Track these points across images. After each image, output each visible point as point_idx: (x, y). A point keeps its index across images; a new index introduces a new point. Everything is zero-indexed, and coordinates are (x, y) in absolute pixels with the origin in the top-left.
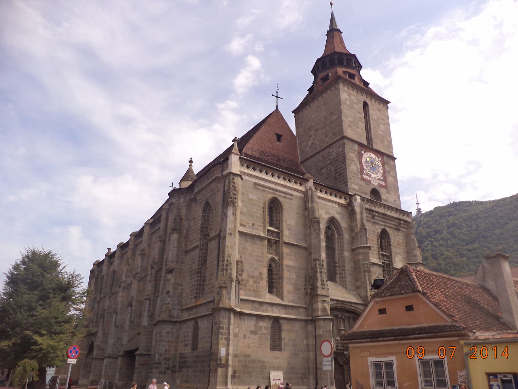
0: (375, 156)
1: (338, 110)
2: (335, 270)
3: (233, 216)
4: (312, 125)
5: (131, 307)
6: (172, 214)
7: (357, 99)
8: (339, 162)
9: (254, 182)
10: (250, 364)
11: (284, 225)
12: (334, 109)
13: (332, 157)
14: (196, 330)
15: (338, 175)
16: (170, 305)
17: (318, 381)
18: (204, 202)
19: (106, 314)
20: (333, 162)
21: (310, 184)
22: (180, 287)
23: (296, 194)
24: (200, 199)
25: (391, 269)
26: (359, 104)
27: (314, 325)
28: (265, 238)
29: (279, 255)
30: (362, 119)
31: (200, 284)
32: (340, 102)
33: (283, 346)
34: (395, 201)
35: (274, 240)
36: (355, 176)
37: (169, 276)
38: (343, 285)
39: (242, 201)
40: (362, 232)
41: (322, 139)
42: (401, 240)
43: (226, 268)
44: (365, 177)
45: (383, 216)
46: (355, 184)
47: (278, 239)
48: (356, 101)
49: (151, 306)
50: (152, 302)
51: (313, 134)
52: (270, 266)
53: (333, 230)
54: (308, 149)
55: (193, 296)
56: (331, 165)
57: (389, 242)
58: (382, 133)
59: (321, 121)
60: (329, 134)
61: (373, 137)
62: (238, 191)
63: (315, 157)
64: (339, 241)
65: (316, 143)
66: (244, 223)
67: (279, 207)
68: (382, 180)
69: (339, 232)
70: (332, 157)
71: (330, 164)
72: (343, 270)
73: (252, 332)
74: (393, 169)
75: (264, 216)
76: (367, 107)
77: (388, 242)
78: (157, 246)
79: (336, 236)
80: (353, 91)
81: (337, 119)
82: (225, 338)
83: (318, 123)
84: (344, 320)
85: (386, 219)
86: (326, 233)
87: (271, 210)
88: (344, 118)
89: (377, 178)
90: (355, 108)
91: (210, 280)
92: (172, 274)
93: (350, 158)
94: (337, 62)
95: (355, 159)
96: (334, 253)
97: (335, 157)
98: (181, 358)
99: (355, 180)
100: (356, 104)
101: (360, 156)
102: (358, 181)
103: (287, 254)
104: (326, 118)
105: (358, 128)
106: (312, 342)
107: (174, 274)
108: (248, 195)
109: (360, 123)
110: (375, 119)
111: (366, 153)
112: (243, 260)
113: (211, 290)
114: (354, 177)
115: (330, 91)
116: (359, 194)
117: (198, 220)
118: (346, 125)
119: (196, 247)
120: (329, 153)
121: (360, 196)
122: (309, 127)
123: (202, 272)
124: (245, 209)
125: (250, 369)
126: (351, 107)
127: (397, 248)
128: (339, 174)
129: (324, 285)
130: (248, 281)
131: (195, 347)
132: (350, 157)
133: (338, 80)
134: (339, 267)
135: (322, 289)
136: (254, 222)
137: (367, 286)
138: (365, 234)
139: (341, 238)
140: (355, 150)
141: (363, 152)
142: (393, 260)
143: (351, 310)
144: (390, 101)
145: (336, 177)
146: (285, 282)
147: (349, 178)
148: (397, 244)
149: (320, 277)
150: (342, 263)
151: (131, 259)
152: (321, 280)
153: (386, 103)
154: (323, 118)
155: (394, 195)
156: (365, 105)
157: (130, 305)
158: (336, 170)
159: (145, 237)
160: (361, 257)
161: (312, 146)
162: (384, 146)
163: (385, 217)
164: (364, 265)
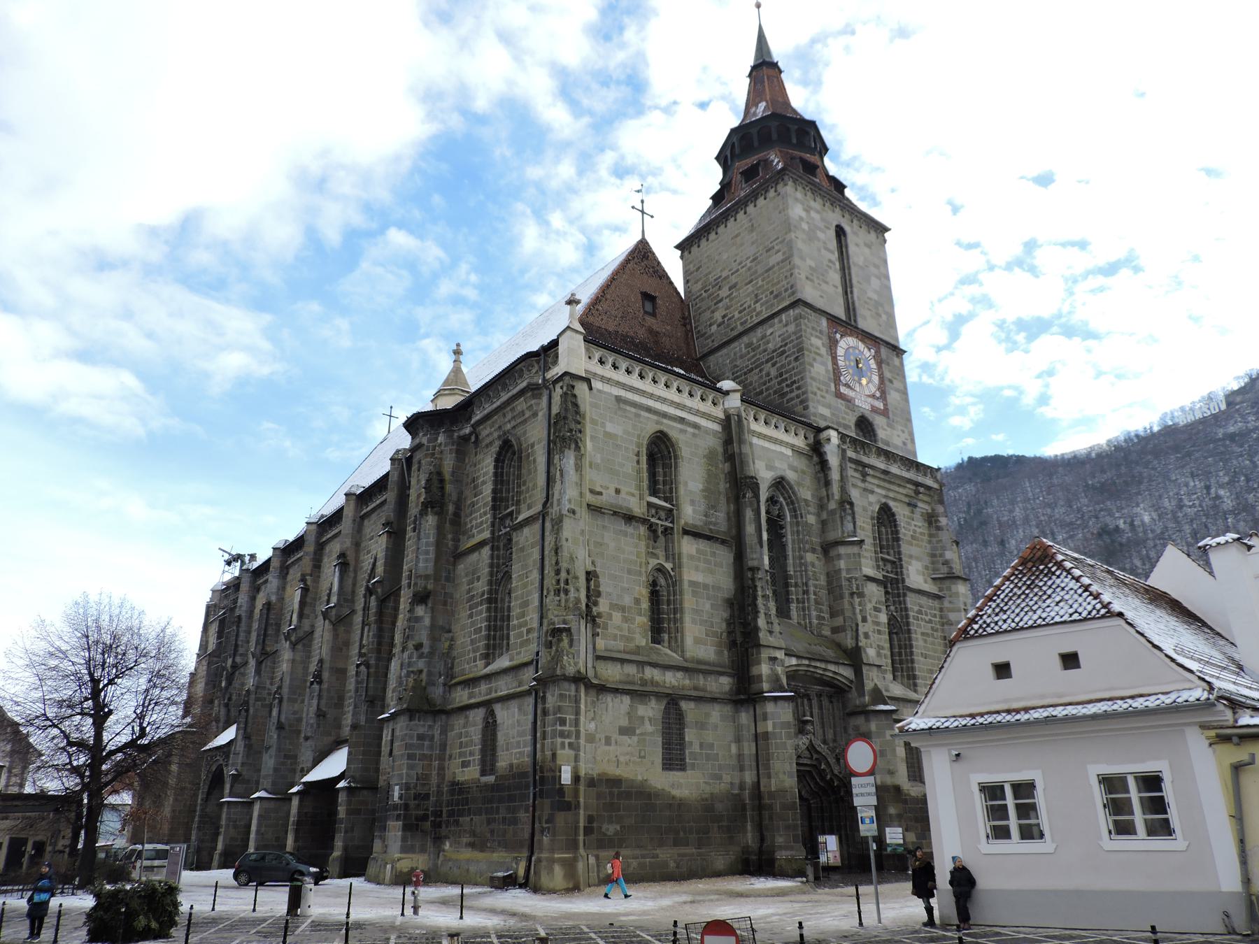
0: (863, 346)
1: (781, 242)
2: (788, 593)
3: (577, 471)
4: (723, 276)
5: (320, 683)
6: (419, 470)
7: (823, 220)
8: (787, 357)
9: (616, 396)
10: (622, 802)
11: (682, 491)
12: (775, 240)
13: (770, 345)
14: (490, 727)
15: (787, 386)
16: (424, 676)
17: (765, 833)
18: (498, 443)
19: (251, 702)
20: (772, 358)
21: (734, 402)
22: (446, 635)
23: (705, 425)
24: (488, 435)
25: (901, 591)
26: (828, 231)
27: (752, 712)
28: (644, 521)
29: (674, 559)
30: (834, 264)
31: (495, 626)
32: (789, 224)
33: (687, 760)
34: (904, 444)
35: (662, 526)
36: (824, 388)
37: (420, 611)
38: (806, 623)
39: (592, 437)
40: (845, 510)
41: (746, 305)
42: (920, 527)
43: (566, 587)
44: (843, 390)
45: (882, 476)
46: (823, 406)
47: (671, 525)
48: (821, 225)
49: (372, 679)
50: (372, 670)
51: (725, 295)
52: (654, 584)
53: (781, 505)
54: (714, 328)
55: (478, 654)
56: (770, 364)
57: (897, 532)
58: (875, 297)
59: (743, 267)
60: (764, 296)
62: (584, 415)
63: (733, 345)
64: (795, 529)
65: (733, 316)
66: (598, 489)
67: (669, 452)
68: (878, 398)
69: (795, 511)
70: (771, 346)
71: (767, 361)
72: (804, 594)
73: (624, 731)
74: (898, 375)
75: (639, 472)
76: (843, 238)
77: (892, 531)
78: (377, 546)
79: (789, 519)
80: (815, 200)
81: (783, 261)
82: (570, 744)
83: (738, 270)
84: (809, 700)
85: (890, 482)
86: (768, 512)
87: (652, 458)
88: (796, 260)
90: (819, 240)
91: (523, 615)
92: (426, 605)
93: (813, 349)
94: (775, 136)
95: (823, 351)
96: (785, 557)
97: (779, 346)
98: (452, 792)
99: (822, 396)
101: (833, 344)
102: (831, 399)
103: (691, 557)
104: (754, 260)
106: (749, 749)
107: (430, 605)
108: (603, 425)
109: (829, 270)
110: (861, 264)
111: (845, 339)
112: (598, 570)
113: (525, 638)
114: (822, 391)
115: (765, 199)
116: (835, 427)
117: (484, 483)
118: (803, 276)
119: (481, 544)
120: (764, 337)
121: (837, 430)
122: (715, 280)
123: (499, 599)
124: (599, 456)
125: (622, 813)
126: (811, 237)
127: (912, 545)
128: (789, 382)
129: (772, 623)
130: (610, 616)
131: (488, 764)
132: (811, 345)
133: (784, 175)
134: (796, 585)
135: (768, 634)
136: (618, 487)
137: (857, 625)
138: (849, 514)
139: (798, 524)
140: (821, 332)
141: (838, 336)
142: (905, 571)
143: (825, 678)
144: (889, 227)
145: (783, 387)
146: (687, 619)
147: (812, 393)
149: (763, 607)
150: (802, 579)
151: (311, 575)
152: (766, 614)
153: (881, 229)
154: (748, 261)
155: (903, 432)
156: (840, 232)
157: (318, 678)
158: (781, 375)
159: (346, 525)
160: (842, 564)
161: (724, 322)
162: (880, 326)
163: (887, 478)
164: (849, 580)
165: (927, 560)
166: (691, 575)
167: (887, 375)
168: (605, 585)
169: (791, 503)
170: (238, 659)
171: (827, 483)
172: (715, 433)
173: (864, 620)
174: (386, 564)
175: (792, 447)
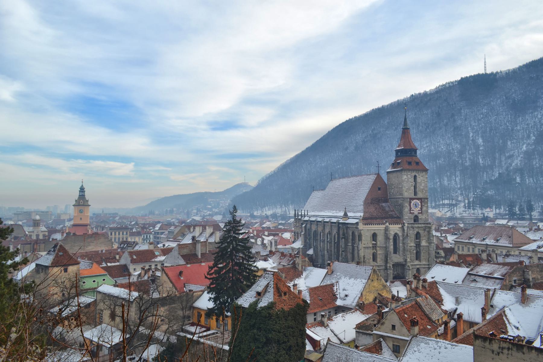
11: (378, 240)
21: (387, 224)
37: (343, 253)
44: (411, 212)
86: (394, 238)
89: (417, 210)
95: (408, 205)
100: (410, 179)
101: (410, 203)
102: (408, 215)
106: (386, 275)
160: (405, 246)
165: (427, 239)
166: (379, 252)
167: (423, 204)
168: (366, 257)
169: (398, 236)
171: (404, 232)
172: (384, 229)
173: (408, 255)
175: (399, 227)
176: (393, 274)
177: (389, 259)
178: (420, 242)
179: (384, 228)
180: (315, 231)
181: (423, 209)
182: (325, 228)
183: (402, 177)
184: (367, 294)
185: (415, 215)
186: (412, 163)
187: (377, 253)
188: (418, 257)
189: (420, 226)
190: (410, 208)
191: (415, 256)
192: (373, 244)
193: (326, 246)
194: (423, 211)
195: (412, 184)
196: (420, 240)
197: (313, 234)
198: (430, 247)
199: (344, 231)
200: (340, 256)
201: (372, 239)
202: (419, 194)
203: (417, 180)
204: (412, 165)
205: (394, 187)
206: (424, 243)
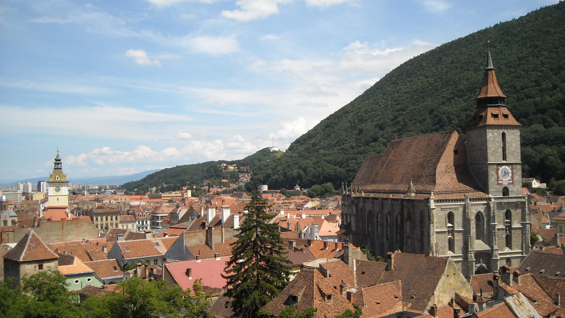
11: (455, 222)
26: (499, 137)
36: (493, 184)
37: (408, 240)
44: (499, 182)
61: (507, 155)
88: (488, 151)
95: (494, 173)
100: (497, 137)
101: (498, 170)
103: (456, 235)
105: (497, 153)
110: (510, 141)
140: (494, 169)
141: (499, 167)
148: (516, 214)
155: (518, 186)
160: (492, 229)
166: (456, 238)
167: (514, 171)
168: (439, 244)
170: (363, 219)
174: (400, 222)
176: (475, 266)
177: (469, 247)
178: (510, 223)
179: (463, 206)
180: (370, 211)
181: (514, 179)
182: (384, 206)
183: (486, 136)
184: (441, 294)
185: (504, 186)
186: (499, 116)
187: (454, 239)
188: (509, 243)
189: (511, 200)
190: (498, 178)
191: (504, 241)
192: (449, 227)
193: (385, 231)
194: (514, 181)
195: (500, 144)
196: (511, 220)
197: (368, 215)
198: (524, 229)
199: (409, 210)
200: (405, 244)
201: (447, 220)
202: (509, 158)
203: (506, 139)
204: (499, 119)
205: (476, 149)
206: (516, 225)
